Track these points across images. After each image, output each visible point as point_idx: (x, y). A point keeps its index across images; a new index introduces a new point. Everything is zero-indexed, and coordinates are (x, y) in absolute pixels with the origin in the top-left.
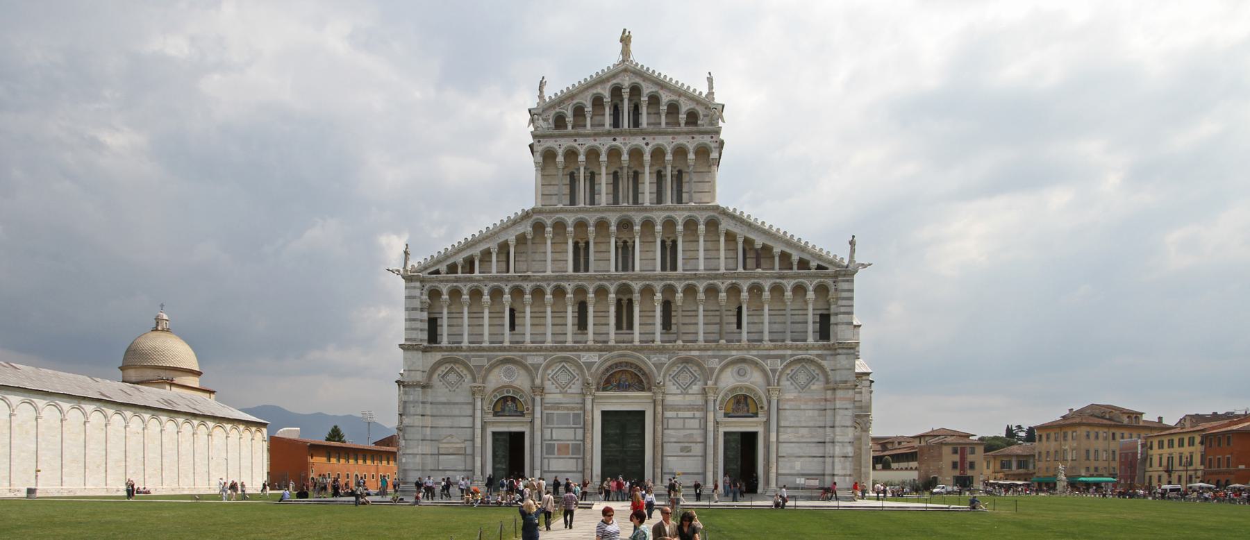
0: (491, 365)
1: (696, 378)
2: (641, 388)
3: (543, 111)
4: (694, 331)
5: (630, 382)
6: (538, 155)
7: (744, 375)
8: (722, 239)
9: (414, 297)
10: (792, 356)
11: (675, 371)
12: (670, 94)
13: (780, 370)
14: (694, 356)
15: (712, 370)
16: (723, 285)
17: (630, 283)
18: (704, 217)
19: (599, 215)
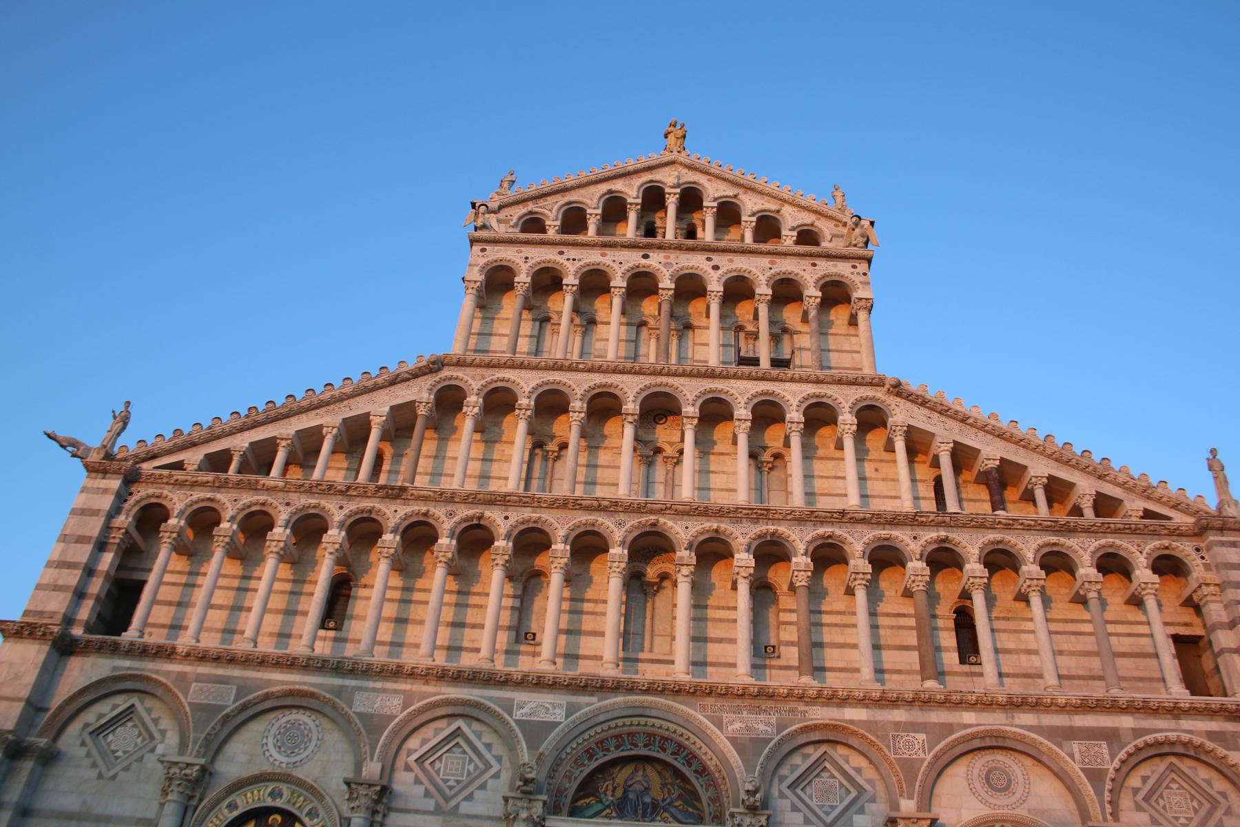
0: (244, 707)
1: (860, 790)
2: (691, 815)
3: (501, 207)
4: (841, 665)
5: (660, 798)
6: (476, 269)
7: (1006, 788)
8: (900, 445)
9: (95, 513)
10: (1138, 733)
11: (798, 766)
12: (762, 201)
13: (1111, 774)
14: (851, 722)
15: (909, 767)
16: (913, 543)
17: (670, 523)
18: (852, 400)
19: (598, 379)
